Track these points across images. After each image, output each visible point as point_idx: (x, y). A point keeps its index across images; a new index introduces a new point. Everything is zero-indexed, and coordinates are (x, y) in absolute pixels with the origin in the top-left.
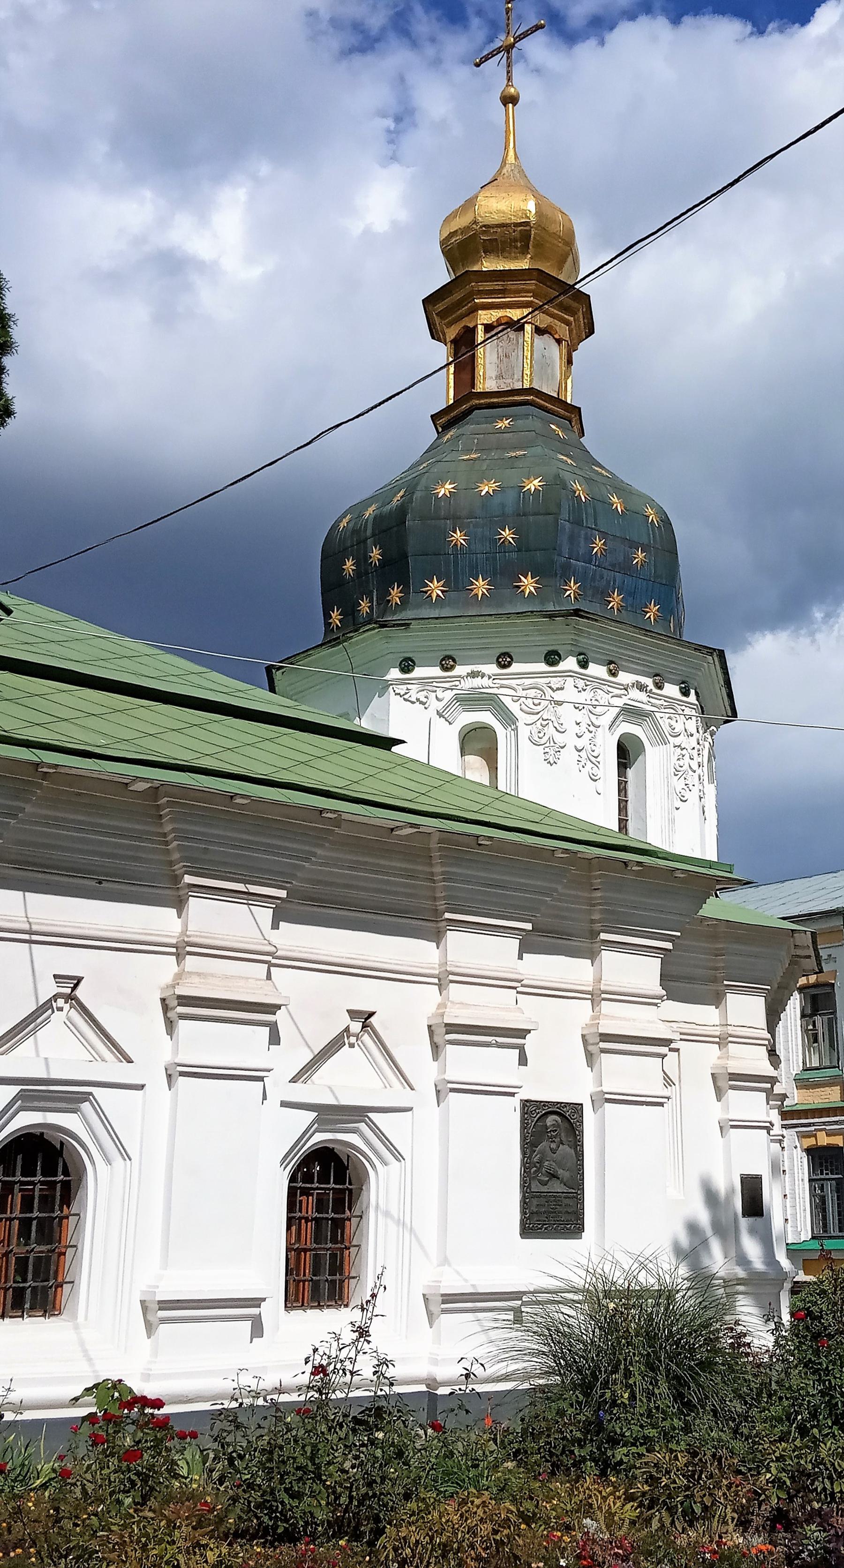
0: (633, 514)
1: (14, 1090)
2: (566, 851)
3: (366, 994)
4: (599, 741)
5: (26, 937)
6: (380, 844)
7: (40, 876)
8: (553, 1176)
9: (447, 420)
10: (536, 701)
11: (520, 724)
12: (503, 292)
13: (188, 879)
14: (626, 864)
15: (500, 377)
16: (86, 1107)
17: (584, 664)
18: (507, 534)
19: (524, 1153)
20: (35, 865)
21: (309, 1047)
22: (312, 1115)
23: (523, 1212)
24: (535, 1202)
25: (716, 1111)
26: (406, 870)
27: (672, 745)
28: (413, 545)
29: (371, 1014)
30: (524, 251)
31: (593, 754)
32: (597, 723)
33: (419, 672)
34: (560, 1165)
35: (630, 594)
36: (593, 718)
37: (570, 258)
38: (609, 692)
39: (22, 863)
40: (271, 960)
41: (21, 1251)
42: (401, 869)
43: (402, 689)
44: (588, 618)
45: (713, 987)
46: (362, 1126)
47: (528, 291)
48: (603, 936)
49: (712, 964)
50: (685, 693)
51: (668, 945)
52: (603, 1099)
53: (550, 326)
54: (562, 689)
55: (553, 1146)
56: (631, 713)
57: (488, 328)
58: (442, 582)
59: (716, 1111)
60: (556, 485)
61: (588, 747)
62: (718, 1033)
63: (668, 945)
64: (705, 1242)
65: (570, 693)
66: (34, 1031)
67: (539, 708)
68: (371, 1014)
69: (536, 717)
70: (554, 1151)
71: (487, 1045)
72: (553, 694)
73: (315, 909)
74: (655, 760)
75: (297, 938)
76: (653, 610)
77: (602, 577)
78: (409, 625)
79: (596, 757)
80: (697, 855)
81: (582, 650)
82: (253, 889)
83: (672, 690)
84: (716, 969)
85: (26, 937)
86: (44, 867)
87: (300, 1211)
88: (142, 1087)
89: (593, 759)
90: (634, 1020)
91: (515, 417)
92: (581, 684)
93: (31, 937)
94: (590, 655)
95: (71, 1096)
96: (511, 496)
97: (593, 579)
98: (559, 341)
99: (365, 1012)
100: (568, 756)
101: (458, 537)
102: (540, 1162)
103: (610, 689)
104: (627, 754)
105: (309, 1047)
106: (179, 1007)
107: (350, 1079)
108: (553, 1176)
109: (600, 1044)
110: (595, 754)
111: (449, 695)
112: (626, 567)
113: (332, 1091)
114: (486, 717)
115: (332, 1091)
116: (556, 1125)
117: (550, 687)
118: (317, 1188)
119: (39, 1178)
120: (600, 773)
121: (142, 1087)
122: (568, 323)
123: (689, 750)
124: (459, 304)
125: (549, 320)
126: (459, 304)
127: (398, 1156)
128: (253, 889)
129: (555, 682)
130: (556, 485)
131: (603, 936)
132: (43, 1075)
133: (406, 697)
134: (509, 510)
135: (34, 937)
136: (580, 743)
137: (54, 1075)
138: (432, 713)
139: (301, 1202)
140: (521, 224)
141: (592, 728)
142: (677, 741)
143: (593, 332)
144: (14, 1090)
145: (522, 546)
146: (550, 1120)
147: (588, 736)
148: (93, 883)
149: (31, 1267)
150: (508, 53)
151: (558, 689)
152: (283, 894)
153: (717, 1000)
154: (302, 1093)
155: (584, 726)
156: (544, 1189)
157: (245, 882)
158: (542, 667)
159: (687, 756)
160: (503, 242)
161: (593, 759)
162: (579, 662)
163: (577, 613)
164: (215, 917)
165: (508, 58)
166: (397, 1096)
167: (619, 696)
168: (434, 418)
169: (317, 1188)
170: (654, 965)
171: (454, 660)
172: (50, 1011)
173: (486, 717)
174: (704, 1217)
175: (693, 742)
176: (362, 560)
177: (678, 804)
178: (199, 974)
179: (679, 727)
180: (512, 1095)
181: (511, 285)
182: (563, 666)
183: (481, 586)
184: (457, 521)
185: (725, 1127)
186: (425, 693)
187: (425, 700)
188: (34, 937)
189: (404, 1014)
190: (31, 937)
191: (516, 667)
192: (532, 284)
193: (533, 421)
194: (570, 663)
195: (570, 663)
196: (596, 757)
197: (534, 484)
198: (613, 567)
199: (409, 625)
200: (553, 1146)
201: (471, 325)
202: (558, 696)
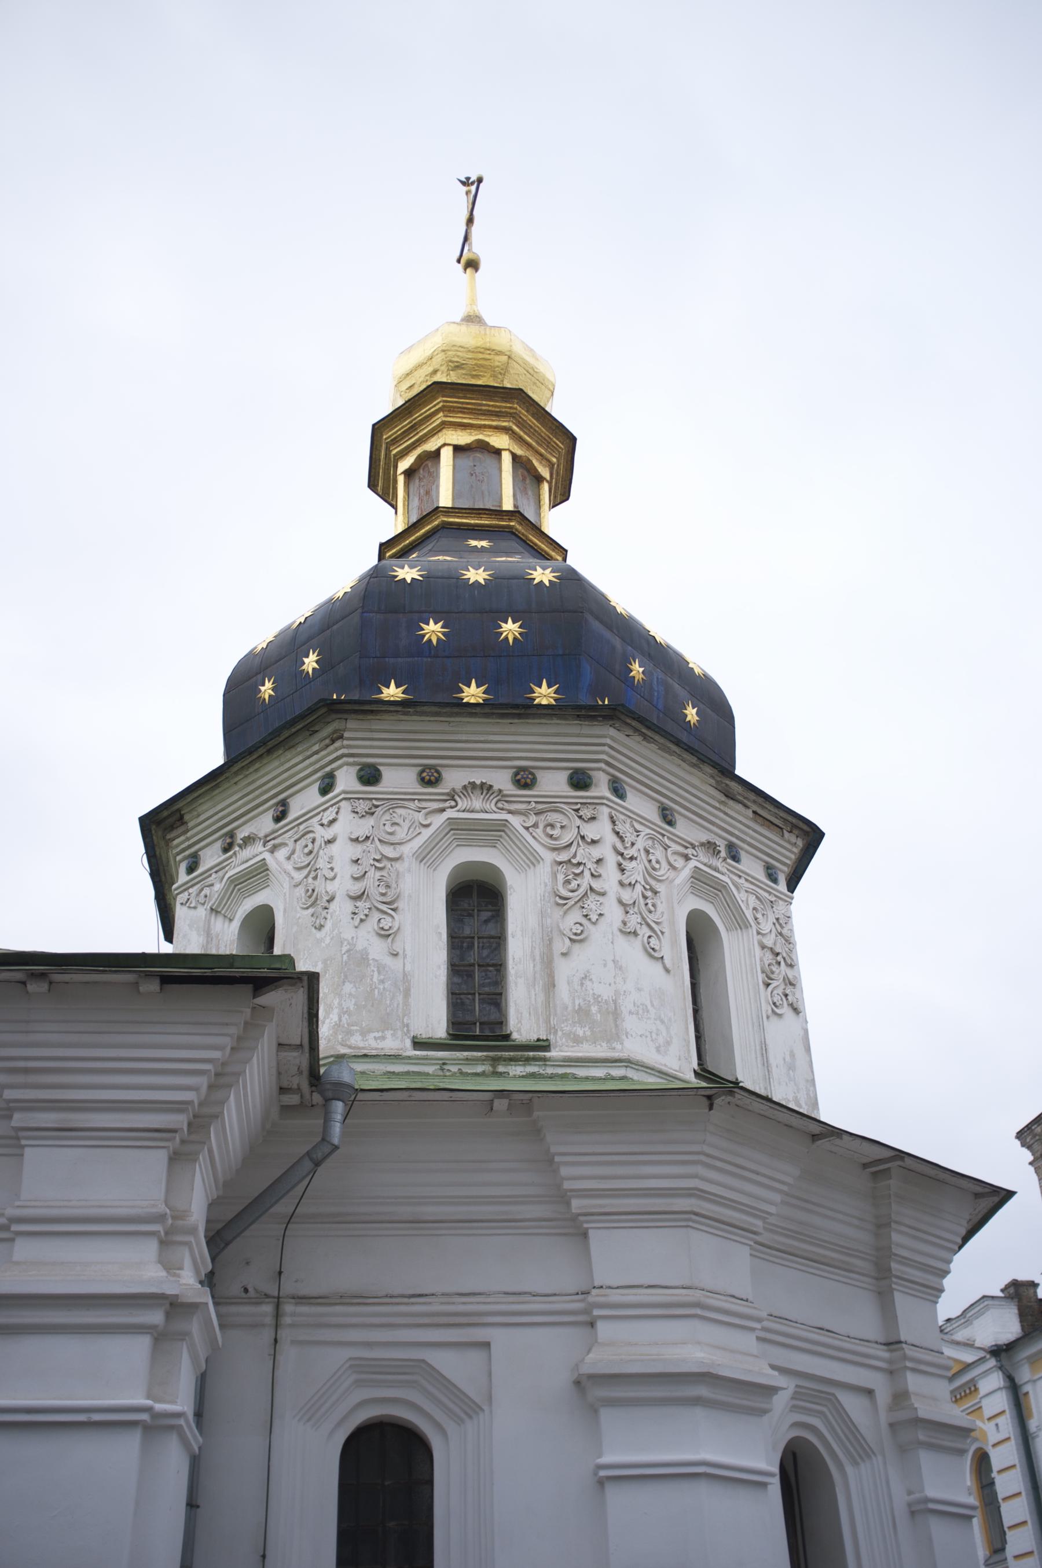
10: (306, 850)
12: (413, 428)
38: (419, 810)
51: (180, 1120)
56: (463, 831)
57: (409, 473)
61: (374, 892)
65: (347, 824)
69: (305, 872)
89: (384, 907)
92: (363, 806)
103: (424, 804)
110: (388, 899)
142: (564, 857)
147: (373, 875)
151: (332, 822)
155: (367, 862)
159: (587, 873)
161: (384, 907)
167: (443, 810)
181: (418, 416)
192: (439, 402)
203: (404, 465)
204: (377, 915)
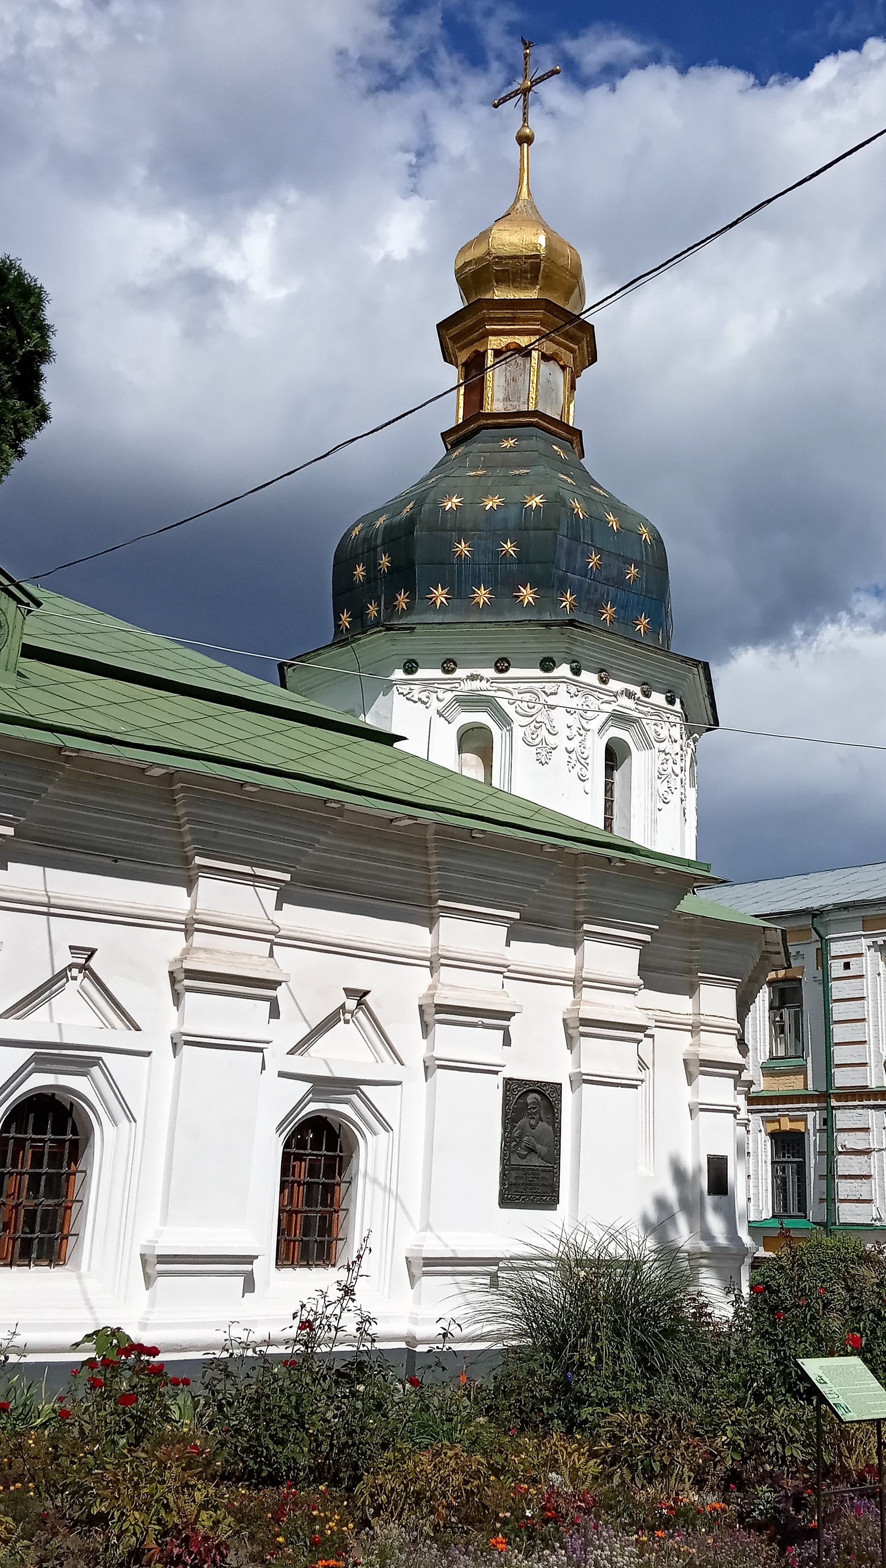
0: (628, 533)
1: (29, 1052)
2: (554, 846)
3: (361, 975)
4: (588, 744)
5: (45, 909)
6: (381, 833)
7: (60, 852)
8: (532, 1150)
9: (455, 438)
10: (531, 705)
11: (515, 726)
12: (513, 320)
13: (198, 860)
14: (609, 860)
15: (507, 399)
16: (95, 1070)
17: (576, 672)
18: (508, 547)
19: (505, 1128)
20: (55, 842)
21: (307, 1022)
22: (308, 1086)
23: (502, 1184)
24: (514, 1174)
25: (686, 1095)
26: (403, 858)
27: (657, 750)
28: (420, 554)
29: (366, 993)
30: (534, 282)
31: (583, 756)
32: (587, 727)
33: (421, 673)
34: (539, 1141)
35: (622, 607)
36: (584, 722)
37: (577, 290)
39: (44, 840)
40: (274, 939)
41: (30, 1204)
42: (398, 858)
43: (405, 689)
44: (582, 628)
45: (687, 978)
46: (354, 1098)
47: (536, 320)
48: (586, 927)
49: (687, 957)
50: (671, 702)
51: (647, 938)
52: (580, 1080)
53: (555, 353)
54: (555, 694)
55: (533, 1122)
56: (619, 718)
57: (497, 353)
58: (446, 590)
59: (686, 1095)
60: (556, 502)
62: (691, 1022)
63: (647, 938)
64: (672, 1217)
65: (562, 698)
66: (49, 998)
67: (533, 711)
68: (366, 993)
69: (530, 720)
70: (533, 1127)
71: (474, 1025)
72: (547, 699)
73: (317, 893)
74: (640, 764)
75: (300, 919)
76: (643, 623)
77: (596, 590)
78: (413, 629)
79: (585, 759)
80: (677, 853)
81: (575, 658)
82: (260, 872)
83: (658, 698)
84: (691, 961)
85: (45, 909)
86: (64, 844)
87: (293, 1175)
88: (148, 1054)
89: (582, 761)
90: (612, 1006)
91: (520, 438)
92: (573, 690)
93: (49, 909)
94: (583, 663)
95: (82, 1060)
96: (513, 511)
97: (588, 592)
98: (563, 368)
99: (361, 991)
100: (559, 757)
101: (463, 548)
102: (520, 1137)
104: (615, 756)
105: (307, 1022)
106: (186, 980)
107: (344, 1053)
108: (532, 1150)
109: (579, 1028)
110: (584, 756)
111: (449, 696)
112: (620, 582)
113: (327, 1064)
114: (483, 718)
115: (327, 1064)
116: (536, 1103)
117: (544, 692)
118: (310, 1155)
119: (49, 1136)
120: (589, 774)
121: (148, 1054)
122: (572, 351)
123: (673, 755)
124: (471, 330)
125: (555, 347)
126: (471, 330)
127: (387, 1127)
128: (260, 872)
129: (549, 687)
130: (556, 502)
131: (586, 927)
132: (56, 1039)
133: (409, 696)
134: (512, 524)
135: (52, 910)
136: (571, 745)
137: (67, 1040)
138: (432, 712)
139: (294, 1166)
140: (531, 257)
141: (582, 732)
142: (662, 746)
143: (596, 361)
144: (29, 1052)
145: (522, 558)
146: (530, 1098)
147: (578, 738)
148: (109, 861)
149: (38, 1219)
150: (525, 96)
151: (552, 694)
152: (287, 877)
153: (691, 990)
154: (297, 1064)
156: (523, 1162)
157: (252, 865)
158: (537, 672)
159: (671, 761)
160: (514, 273)
161: (582, 761)
162: (572, 669)
163: (571, 623)
164: (224, 897)
165: (525, 100)
166: (388, 1070)
168: (444, 435)
169: (310, 1155)
170: (633, 956)
171: (455, 664)
172: (65, 979)
173: (483, 718)
174: (671, 1194)
175: (676, 747)
176: (372, 566)
177: (661, 805)
178: (206, 950)
179: (664, 734)
180: (496, 1073)
181: (520, 313)
182: (557, 672)
183: (482, 595)
184: (462, 533)
185: (694, 1110)
186: (426, 693)
187: (426, 700)
188: (52, 910)
189: (398, 993)
190: (49, 909)
191: (513, 672)
192: (540, 313)
193: (536, 441)
194: (564, 670)
195: (564, 670)
196: (585, 759)
197: (536, 501)
198: (607, 581)
199: (413, 629)
200: (533, 1122)
201: (482, 350)
202: (551, 700)
203: (495, 342)
204: (579, 766)
